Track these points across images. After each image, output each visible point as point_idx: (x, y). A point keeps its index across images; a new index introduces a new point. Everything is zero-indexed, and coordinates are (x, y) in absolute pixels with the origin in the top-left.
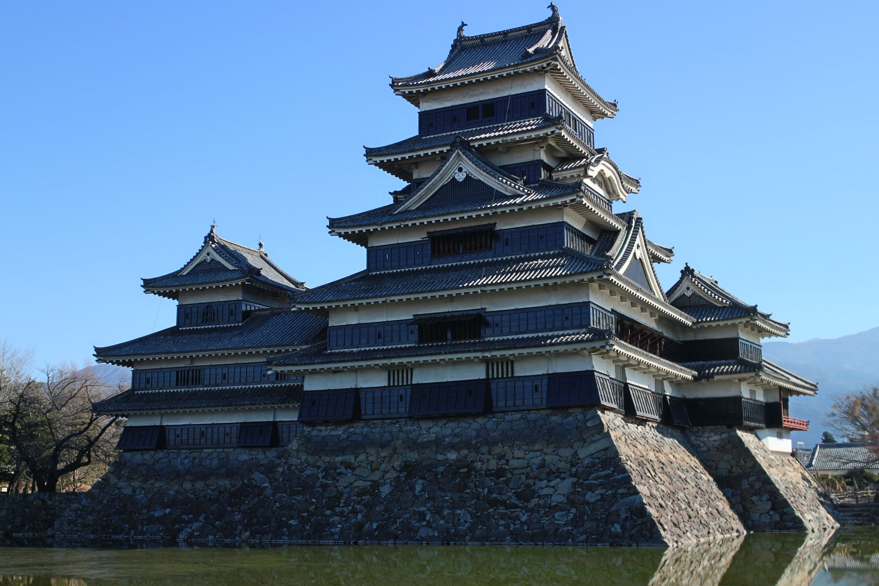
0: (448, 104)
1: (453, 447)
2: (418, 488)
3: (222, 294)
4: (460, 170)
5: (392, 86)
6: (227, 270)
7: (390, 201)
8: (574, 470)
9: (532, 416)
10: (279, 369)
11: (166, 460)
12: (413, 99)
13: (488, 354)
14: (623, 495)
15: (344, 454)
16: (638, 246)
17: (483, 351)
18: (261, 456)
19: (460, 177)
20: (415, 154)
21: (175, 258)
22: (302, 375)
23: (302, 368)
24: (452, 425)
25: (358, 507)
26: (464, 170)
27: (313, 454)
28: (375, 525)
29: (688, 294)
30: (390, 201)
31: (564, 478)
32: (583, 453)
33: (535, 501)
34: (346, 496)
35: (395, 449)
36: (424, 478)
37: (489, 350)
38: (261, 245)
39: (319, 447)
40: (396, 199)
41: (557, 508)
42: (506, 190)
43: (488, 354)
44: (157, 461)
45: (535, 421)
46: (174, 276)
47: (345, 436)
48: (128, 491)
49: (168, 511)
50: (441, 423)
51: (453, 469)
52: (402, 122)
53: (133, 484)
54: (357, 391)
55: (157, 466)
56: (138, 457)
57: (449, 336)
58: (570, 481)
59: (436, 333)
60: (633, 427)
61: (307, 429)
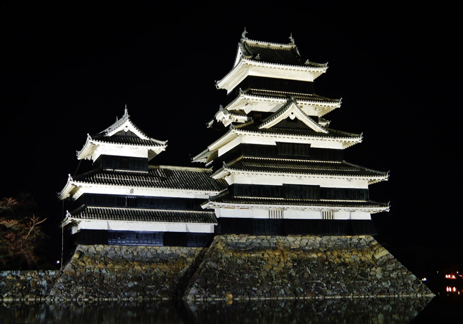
1: (313, 251)
8: (378, 264)
11: (113, 252)
19: (292, 117)
25: (285, 280)
26: (294, 114)
27: (236, 251)
31: (376, 268)
32: (377, 257)
34: (273, 275)
39: (236, 248)
44: (107, 253)
45: (346, 241)
48: (96, 270)
49: (136, 283)
51: (322, 261)
58: (379, 269)
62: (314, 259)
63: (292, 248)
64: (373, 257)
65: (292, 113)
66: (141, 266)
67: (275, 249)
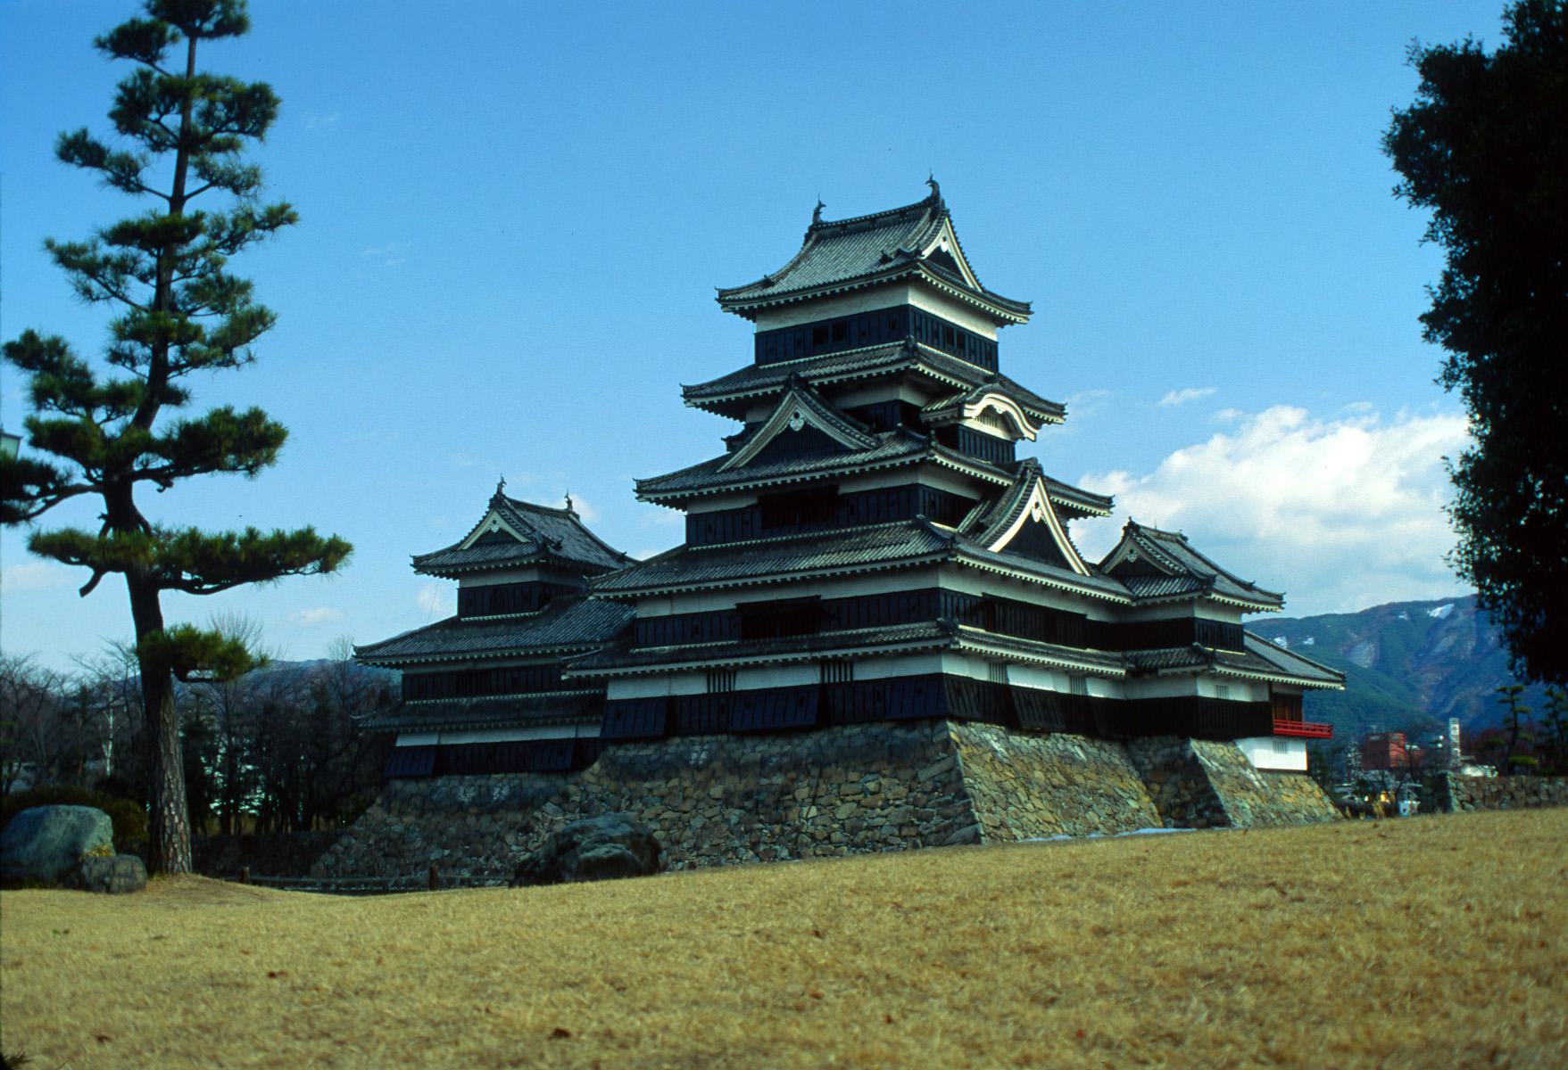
0: (791, 323)
1: (780, 768)
2: (734, 820)
5: (719, 300)
6: (516, 541)
7: (723, 450)
9: (875, 729)
10: (576, 674)
12: (750, 314)
13: (818, 655)
14: (960, 826)
16: (1037, 505)
17: (812, 650)
19: (797, 425)
20: (741, 395)
21: (455, 525)
22: (603, 682)
23: (602, 673)
24: (779, 742)
27: (617, 780)
29: (1132, 558)
30: (723, 450)
33: (862, 834)
36: (742, 808)
37: (820, 650)
38: (569, 503)
40: (730, 447)
43: (818, 655)
46: (454, 550)
47: (654, 757)
48: (398, 828)
49: (447, 852)
50: (768, 740)
52: (733, 347)
54: (671, 700)
55: (435, 797)
56: (411, 787)
59: (766, 625)
60: (1015, 739)
61: (611, 750)
64: (915, 777)
65: (797, 416)
66: (478, 816)
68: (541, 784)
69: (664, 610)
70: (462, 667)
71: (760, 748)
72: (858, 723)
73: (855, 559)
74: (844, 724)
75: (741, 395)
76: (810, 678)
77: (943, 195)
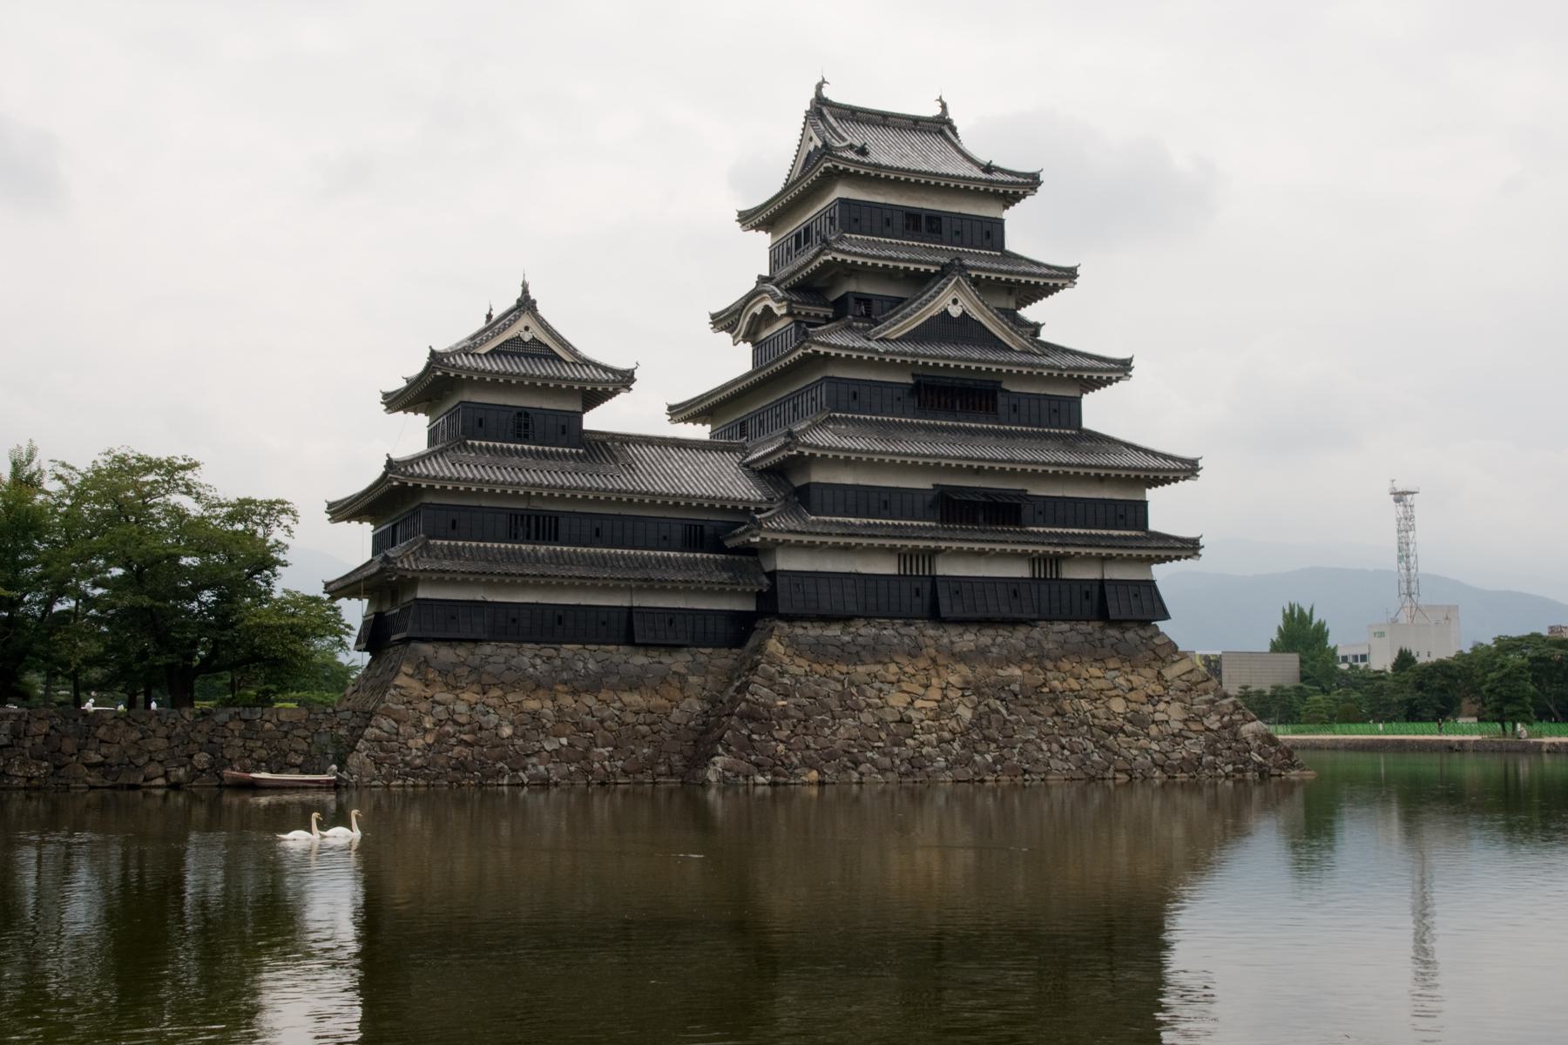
1: (1008, 661)
3: (504, 396)
4: (955, 302)
9: (1084, 627)
10: (770, 536)
15: (864, 663)
18: (666, 660)
19: (955, 311)
24: (991, 632)
28: (989, 758)
35: (934, 661)
41: (1180, 734)
42: (1013, 340)
49: (564, 741)
53: (465, 696)
55: (489, 668)
56: (446, 654)
57: (981, 518)
62: (1011, 680)
63: (957, 649)
65: (955, 302)
66: (575, 692)
67: (914, 652)
68: (640, 659)
69: (847, 478)
70: (523, 506)
71: (969, 636)
72: (1065, 620)
73: (1094, 462)
74: (1050, 620)
75: (891, 264)
76: (1021, 571)
77: (952, 115)
